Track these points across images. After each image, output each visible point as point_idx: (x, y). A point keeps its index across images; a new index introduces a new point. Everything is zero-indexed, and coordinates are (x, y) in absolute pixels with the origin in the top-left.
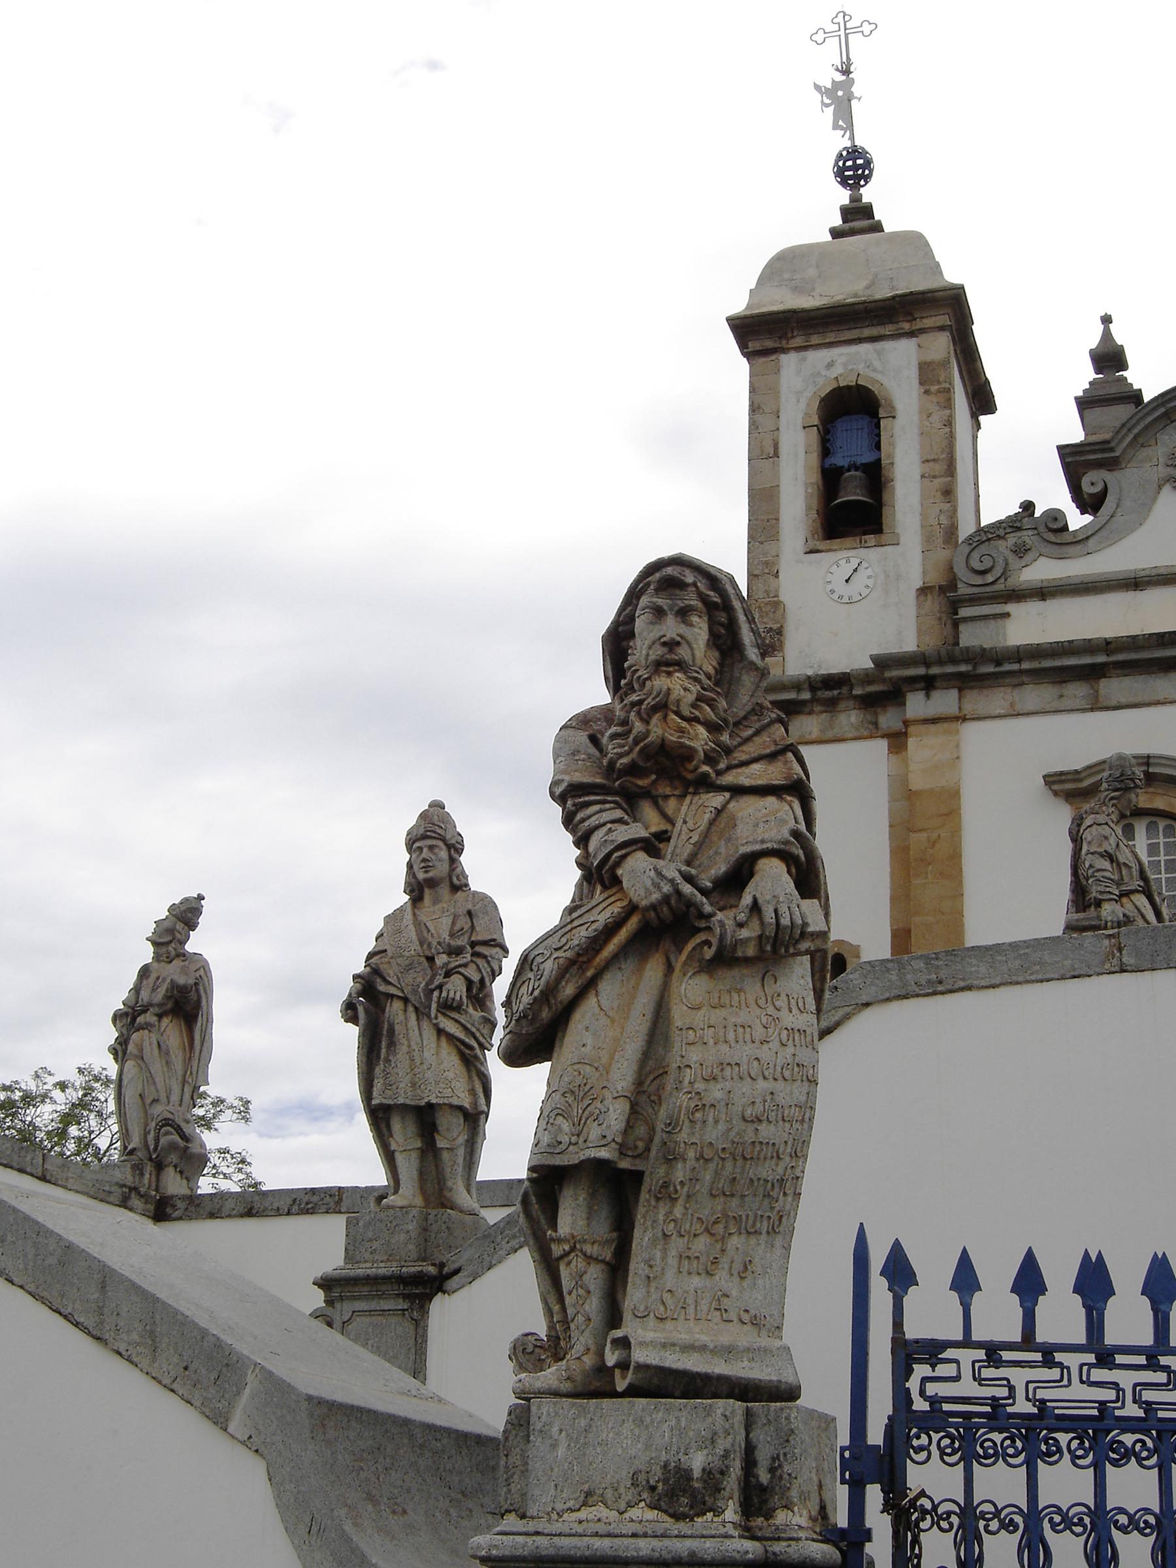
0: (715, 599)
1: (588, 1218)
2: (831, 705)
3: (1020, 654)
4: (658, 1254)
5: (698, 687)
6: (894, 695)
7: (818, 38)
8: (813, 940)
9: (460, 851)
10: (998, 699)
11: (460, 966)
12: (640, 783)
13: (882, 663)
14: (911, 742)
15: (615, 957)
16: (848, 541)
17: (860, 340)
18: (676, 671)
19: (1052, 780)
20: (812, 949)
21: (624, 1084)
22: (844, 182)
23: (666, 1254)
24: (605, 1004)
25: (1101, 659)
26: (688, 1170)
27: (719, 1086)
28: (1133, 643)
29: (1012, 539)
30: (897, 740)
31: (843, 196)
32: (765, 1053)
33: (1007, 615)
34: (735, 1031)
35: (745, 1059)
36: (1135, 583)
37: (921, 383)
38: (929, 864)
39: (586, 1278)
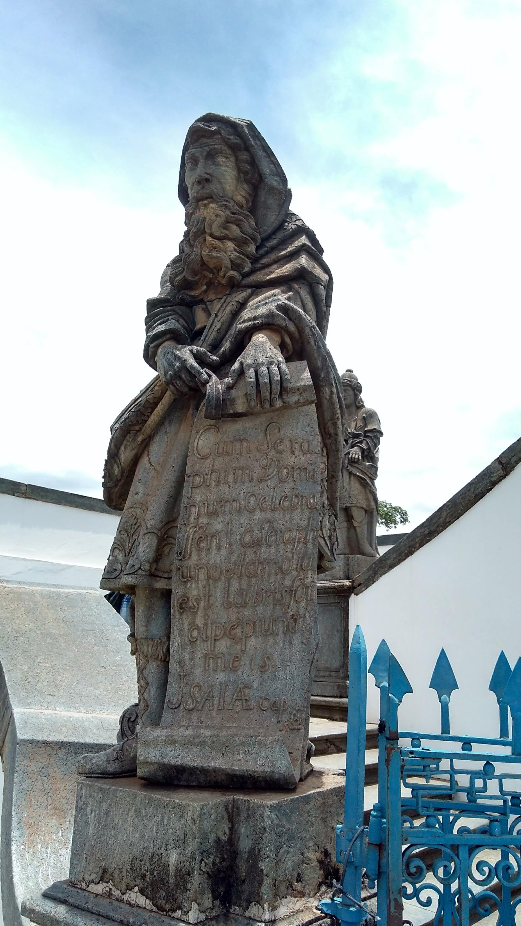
0: (235, 141)
1: (146, 626)
4: (187, 657)
5: (228, 212)
8: (301, 393)
9: (360, 391)
11: (358, 443)
12: (192, 293)
15: (160, 424)
18: (210, 203)
20: (301, 401)
21: (152, 522)
23: (193, 656)
24: (153, 459)
26: (201, 588)
27: (219, 520)
32: (262, 489)
34: (234, 474)
35: (242, 496)
39: (146, 672)
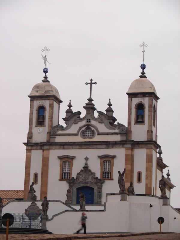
2: (37, 146)
3: (56, 143)
6: (43, 145)
7: (43, 50)
10: (54, 147)
13: (41, 143)
14: (44, 151)
17: (43, 100)
19: (58, 157)
22: (44, 73)
25: (64, 144)
28: (67, 142)
29: (57, 128)
30: (43, 150)
31: (44, 75)
33: (55, 137)
36: (69, 135)
37: (50, 106)
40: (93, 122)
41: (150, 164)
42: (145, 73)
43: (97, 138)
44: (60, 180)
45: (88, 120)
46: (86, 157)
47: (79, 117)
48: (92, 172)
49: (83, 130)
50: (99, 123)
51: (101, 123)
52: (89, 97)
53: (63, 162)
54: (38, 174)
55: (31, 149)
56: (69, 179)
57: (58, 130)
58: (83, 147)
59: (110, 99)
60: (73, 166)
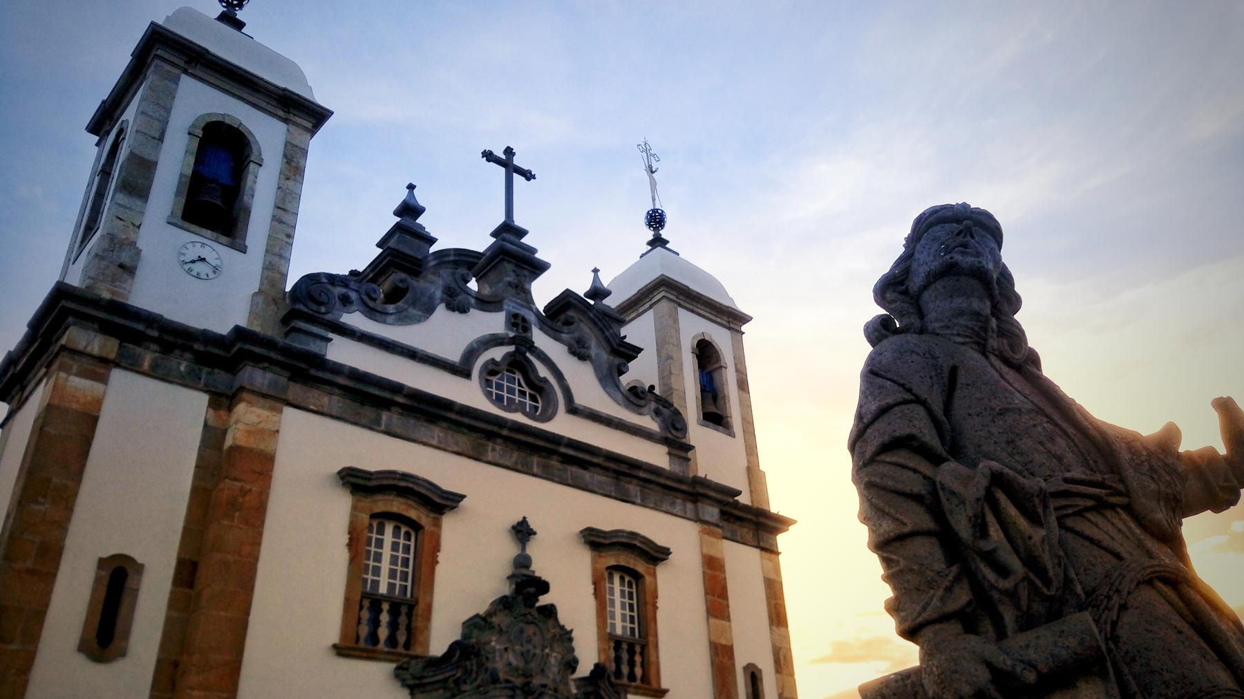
6: (232, 365)
16: (209, 233)
29: (339, 290)
30: (223, 400)
33: (330, 340)
38: (237, 510)
40: (540, 339)
41: (782, 629)
42: (667, 242)
43: (563, 425)
44: (341, 650)
45: (516, 316)
46: (521, 519)
47: (467, 282)
48: (562, 628)
49: (493, 360)
50: (573, 352)
51: (582, 357)
52: (500, 219)
53: (374, 516)
54: (140, 568)
55: (112, 356)
56: (400, 649)
57: (345, 301)
58: (495, 450)
59: (596, 271)
60: (437, 562)
